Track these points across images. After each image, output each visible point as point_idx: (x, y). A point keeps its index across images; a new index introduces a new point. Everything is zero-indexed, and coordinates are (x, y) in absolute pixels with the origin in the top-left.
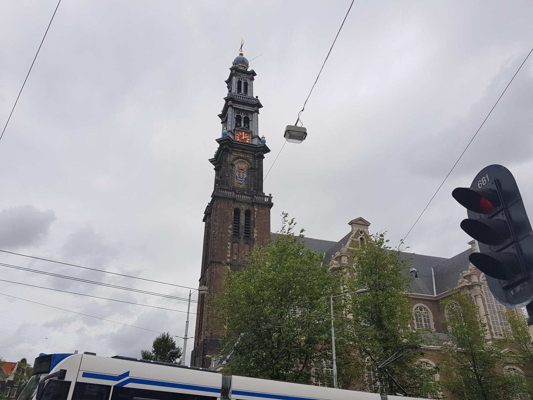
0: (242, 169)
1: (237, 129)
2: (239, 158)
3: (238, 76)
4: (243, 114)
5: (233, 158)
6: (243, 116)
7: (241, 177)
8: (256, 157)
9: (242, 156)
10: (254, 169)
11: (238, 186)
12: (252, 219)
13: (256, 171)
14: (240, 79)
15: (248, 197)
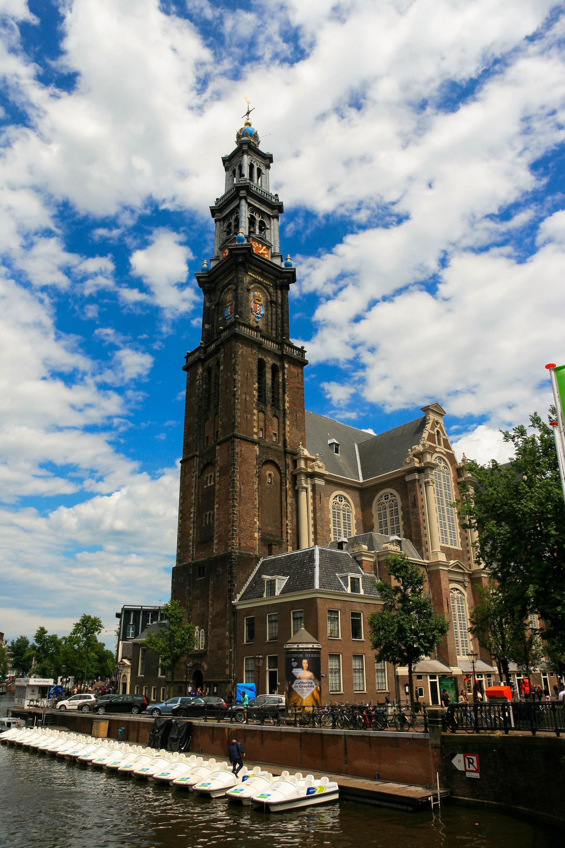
1: (253, 236)
2: (255, 281)
6: (258, 218)
7: (258, 312)
12: (281, 380)
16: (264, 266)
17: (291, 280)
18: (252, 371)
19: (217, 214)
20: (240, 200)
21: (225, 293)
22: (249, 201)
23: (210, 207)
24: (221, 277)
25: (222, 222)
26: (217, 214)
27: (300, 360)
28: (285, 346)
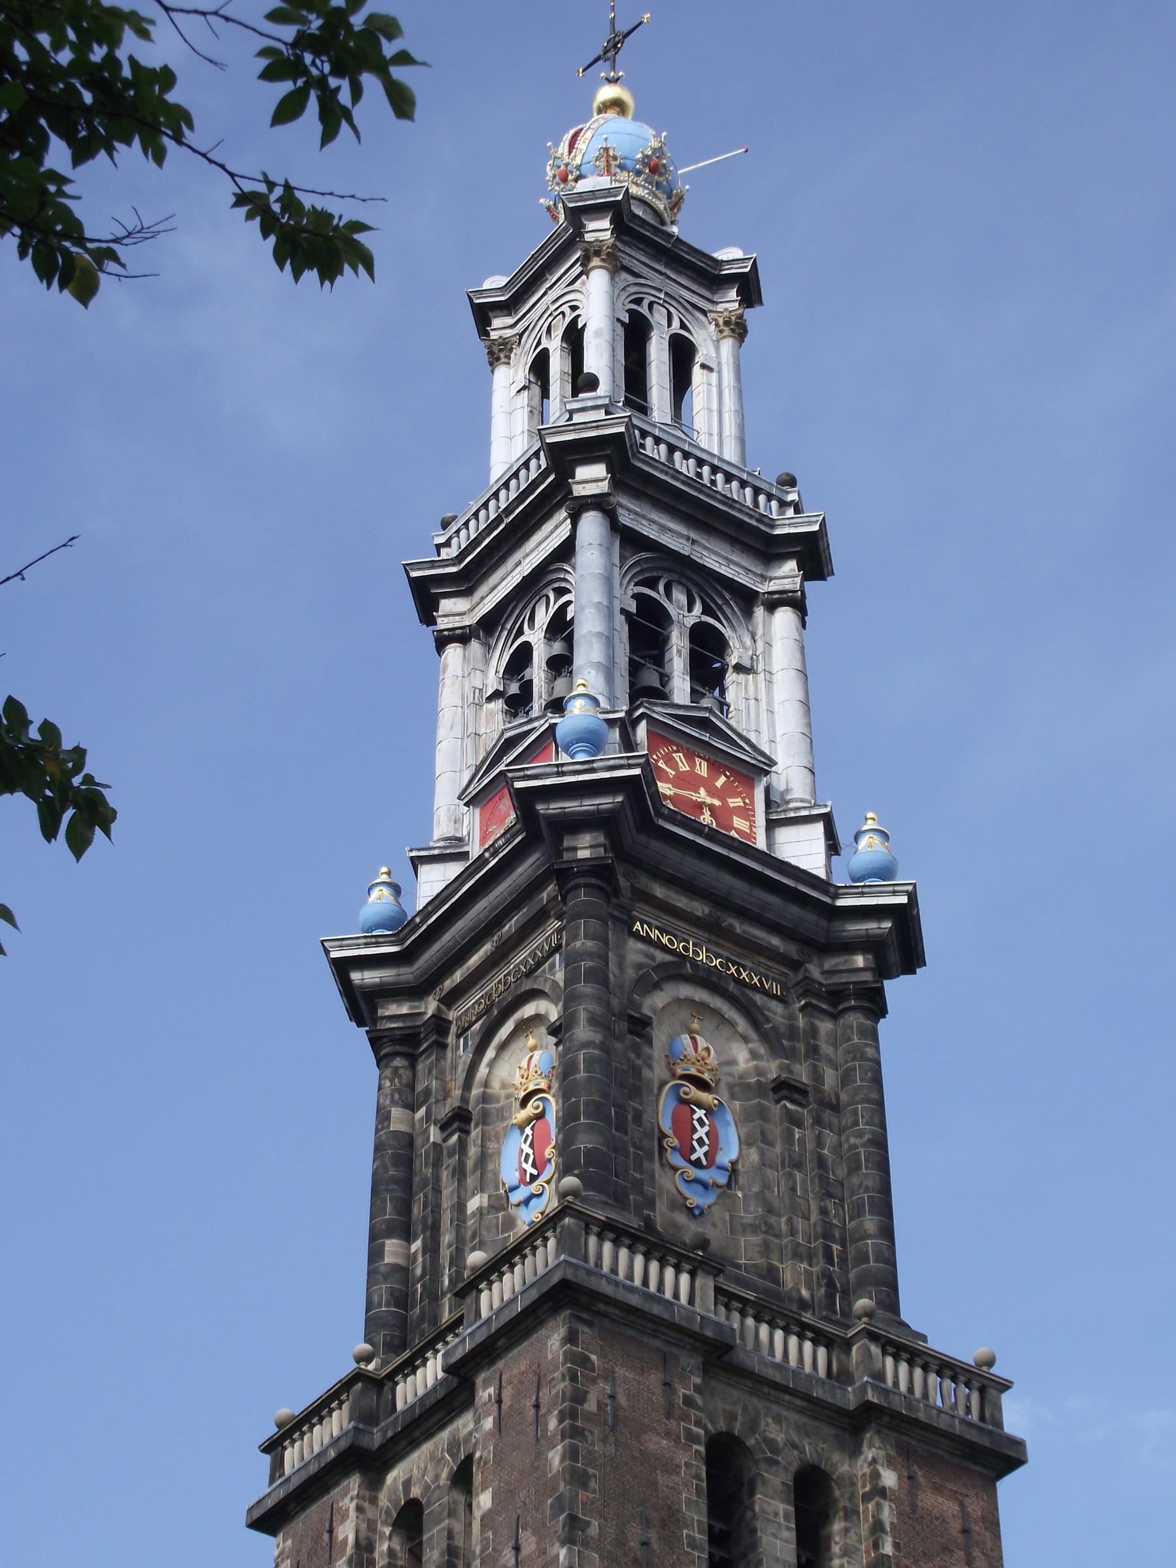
0: (706, 1076)
1: (659, 712)
3: (624, 276)
4: (680, 596)
5: (640, 966)
7: (700, 1153)
8: (818, 995)
9: (702, 957)
10: (804, 1092)
11: (675, 1225)
13: (827, 1115)
14: (638, 301)
15: (808, 1345)
16: (727, 881)
17: (894, 956)
18: (671, 1518)
19: (446, 605)
20: (575, 518)
21: (503, 1046)
22: (625, 519)
23: (407, 568)
24: (475, 960)
25: (475, 645)
26: (446, 605)
27: (972, 1436)
28: (875, 1349)
